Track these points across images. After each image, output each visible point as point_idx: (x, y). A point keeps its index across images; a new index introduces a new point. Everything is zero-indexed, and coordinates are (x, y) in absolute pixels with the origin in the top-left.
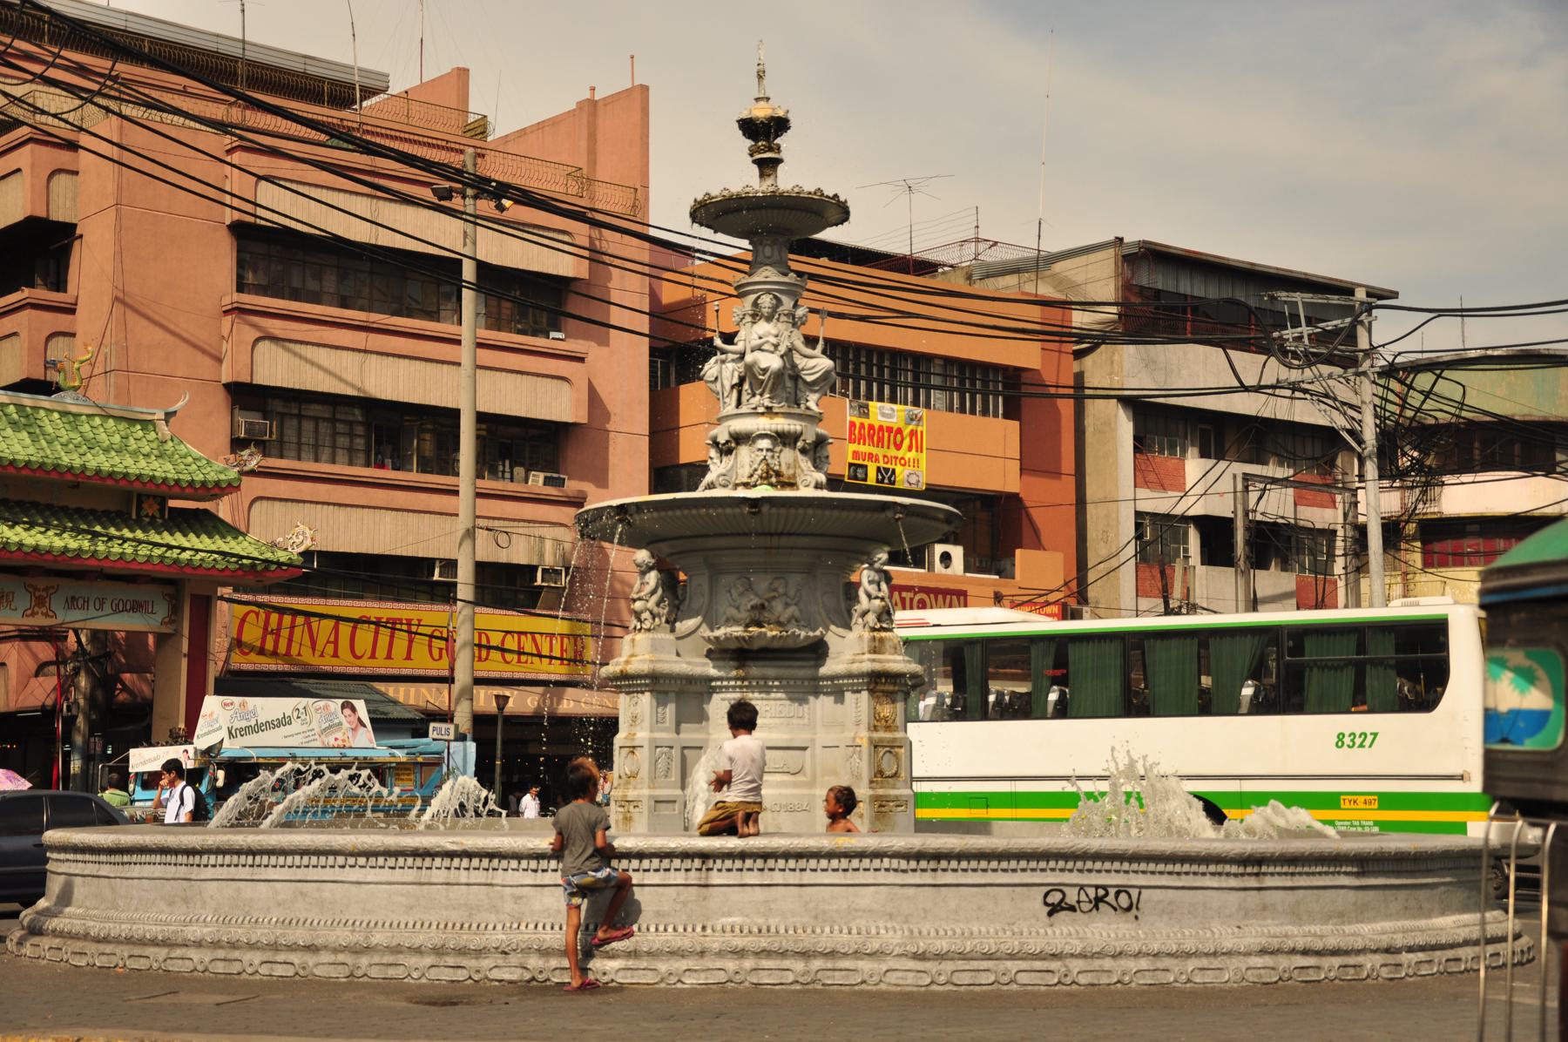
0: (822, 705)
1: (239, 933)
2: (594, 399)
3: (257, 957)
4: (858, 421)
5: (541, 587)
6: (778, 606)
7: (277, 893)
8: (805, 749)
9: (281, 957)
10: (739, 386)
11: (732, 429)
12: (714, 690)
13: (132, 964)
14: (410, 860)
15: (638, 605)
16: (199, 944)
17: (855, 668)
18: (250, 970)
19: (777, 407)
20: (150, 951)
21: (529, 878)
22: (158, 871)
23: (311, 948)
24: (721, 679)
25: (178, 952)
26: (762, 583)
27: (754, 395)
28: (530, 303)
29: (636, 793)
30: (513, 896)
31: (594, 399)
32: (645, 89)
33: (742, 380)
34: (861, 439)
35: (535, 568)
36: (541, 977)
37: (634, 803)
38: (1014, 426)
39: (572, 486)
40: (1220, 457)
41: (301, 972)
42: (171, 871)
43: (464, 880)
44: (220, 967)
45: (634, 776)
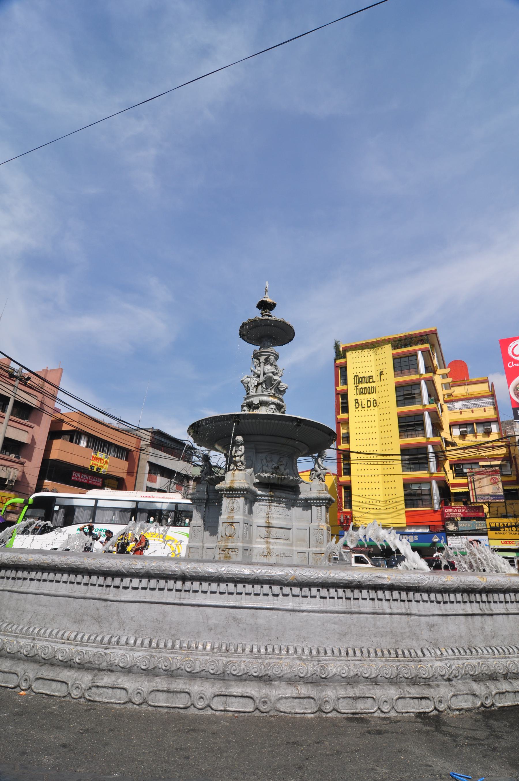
0: (297, 511)
1: (178, 660)
2: (33, 439)
3: (208, 689)
4: (94, 456)
5: (7, 485)
6: (282, 468)
7: (208, 618)
8: (290, 529)
9: (237, 689)
10: (257, 387)
11: (261, 399)
12: (255, 500)
13: (40, 687)
14: (340, 591)
15: (237, 459)
16: (128, 671)
17: (322, 496)
18: (200, 704)
19: (276, 395)
20: (65, 674)
21: (436, 609)
22: (63, 589)
23: (265, 679)
24: (262, 496)
25: (107, 680)
26: (276, 458)
27: (267, 389)
28: (24, 411)
29: (234, 544)
30: (428, 624)
31: (33, 439)
32: (62, 369)
33: (258, 384)
34: (94, 460)
35: (7, 479)
36: (488, 702)
37: (234, 550)
38: (127, 463)
39: (22, 460)
40: (163, 476)
41: (263, 708)
42: (80, 590)
43: (388, 611)
44: (162, 700)
45: (231, 536)
